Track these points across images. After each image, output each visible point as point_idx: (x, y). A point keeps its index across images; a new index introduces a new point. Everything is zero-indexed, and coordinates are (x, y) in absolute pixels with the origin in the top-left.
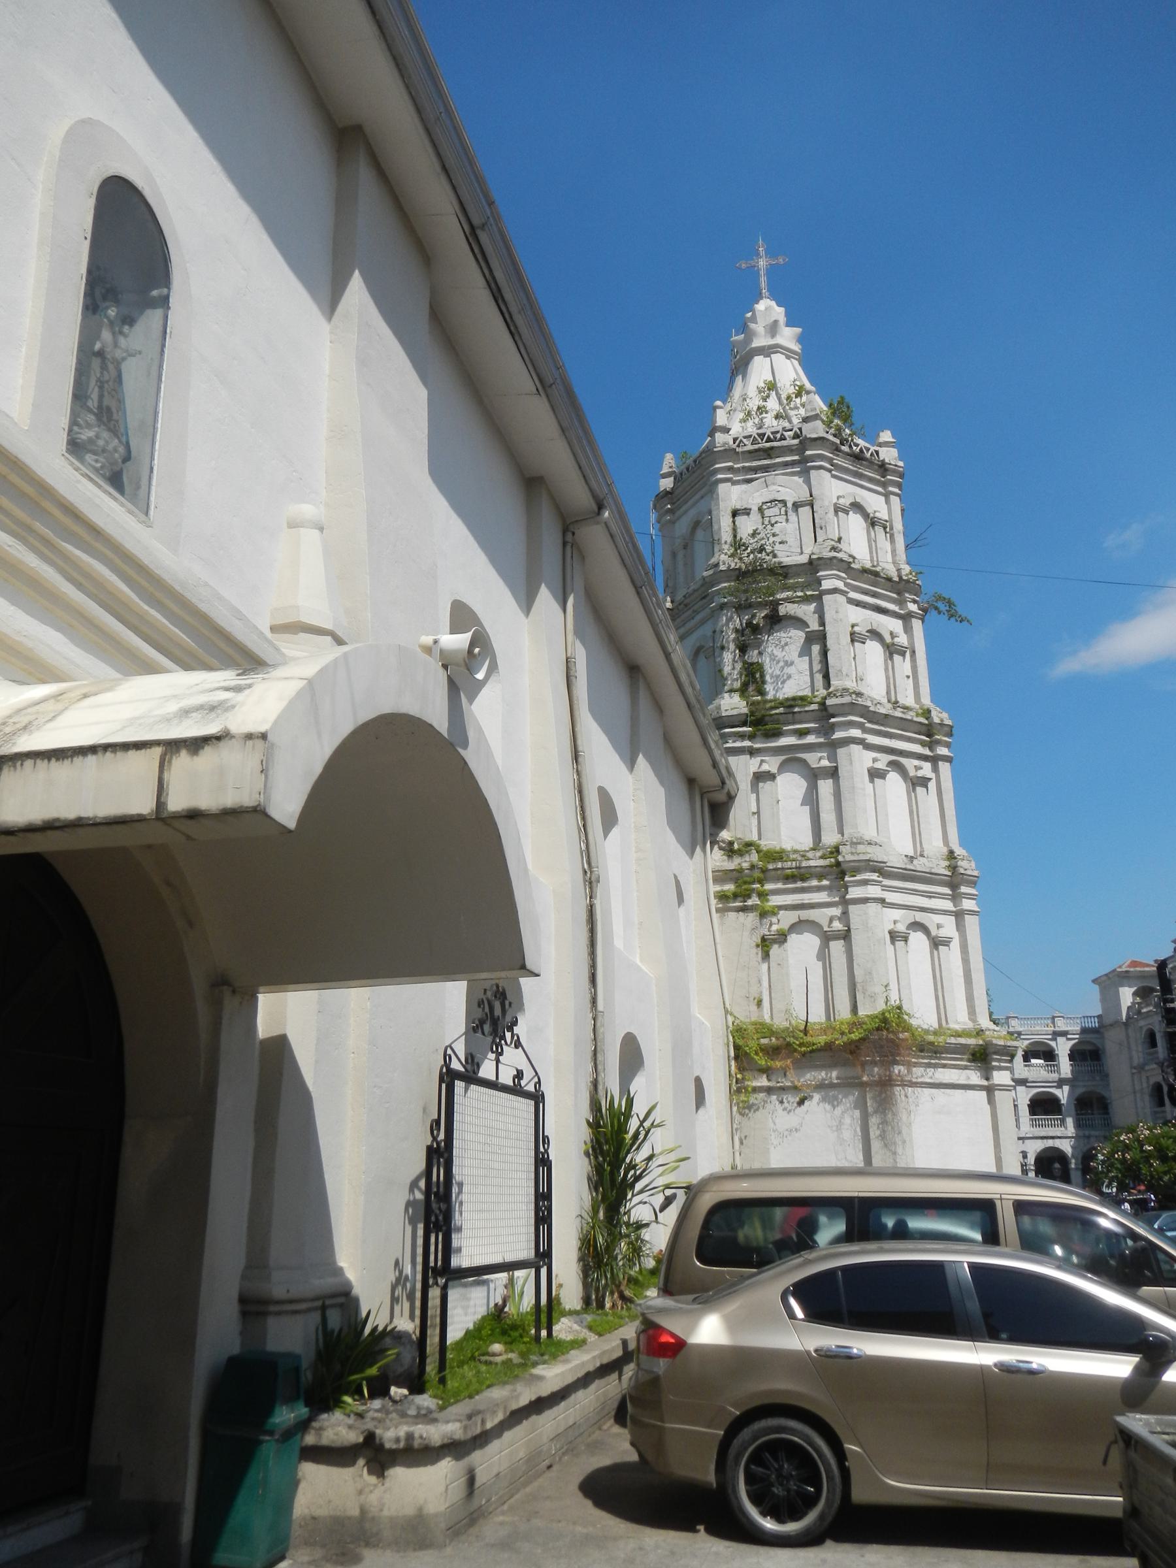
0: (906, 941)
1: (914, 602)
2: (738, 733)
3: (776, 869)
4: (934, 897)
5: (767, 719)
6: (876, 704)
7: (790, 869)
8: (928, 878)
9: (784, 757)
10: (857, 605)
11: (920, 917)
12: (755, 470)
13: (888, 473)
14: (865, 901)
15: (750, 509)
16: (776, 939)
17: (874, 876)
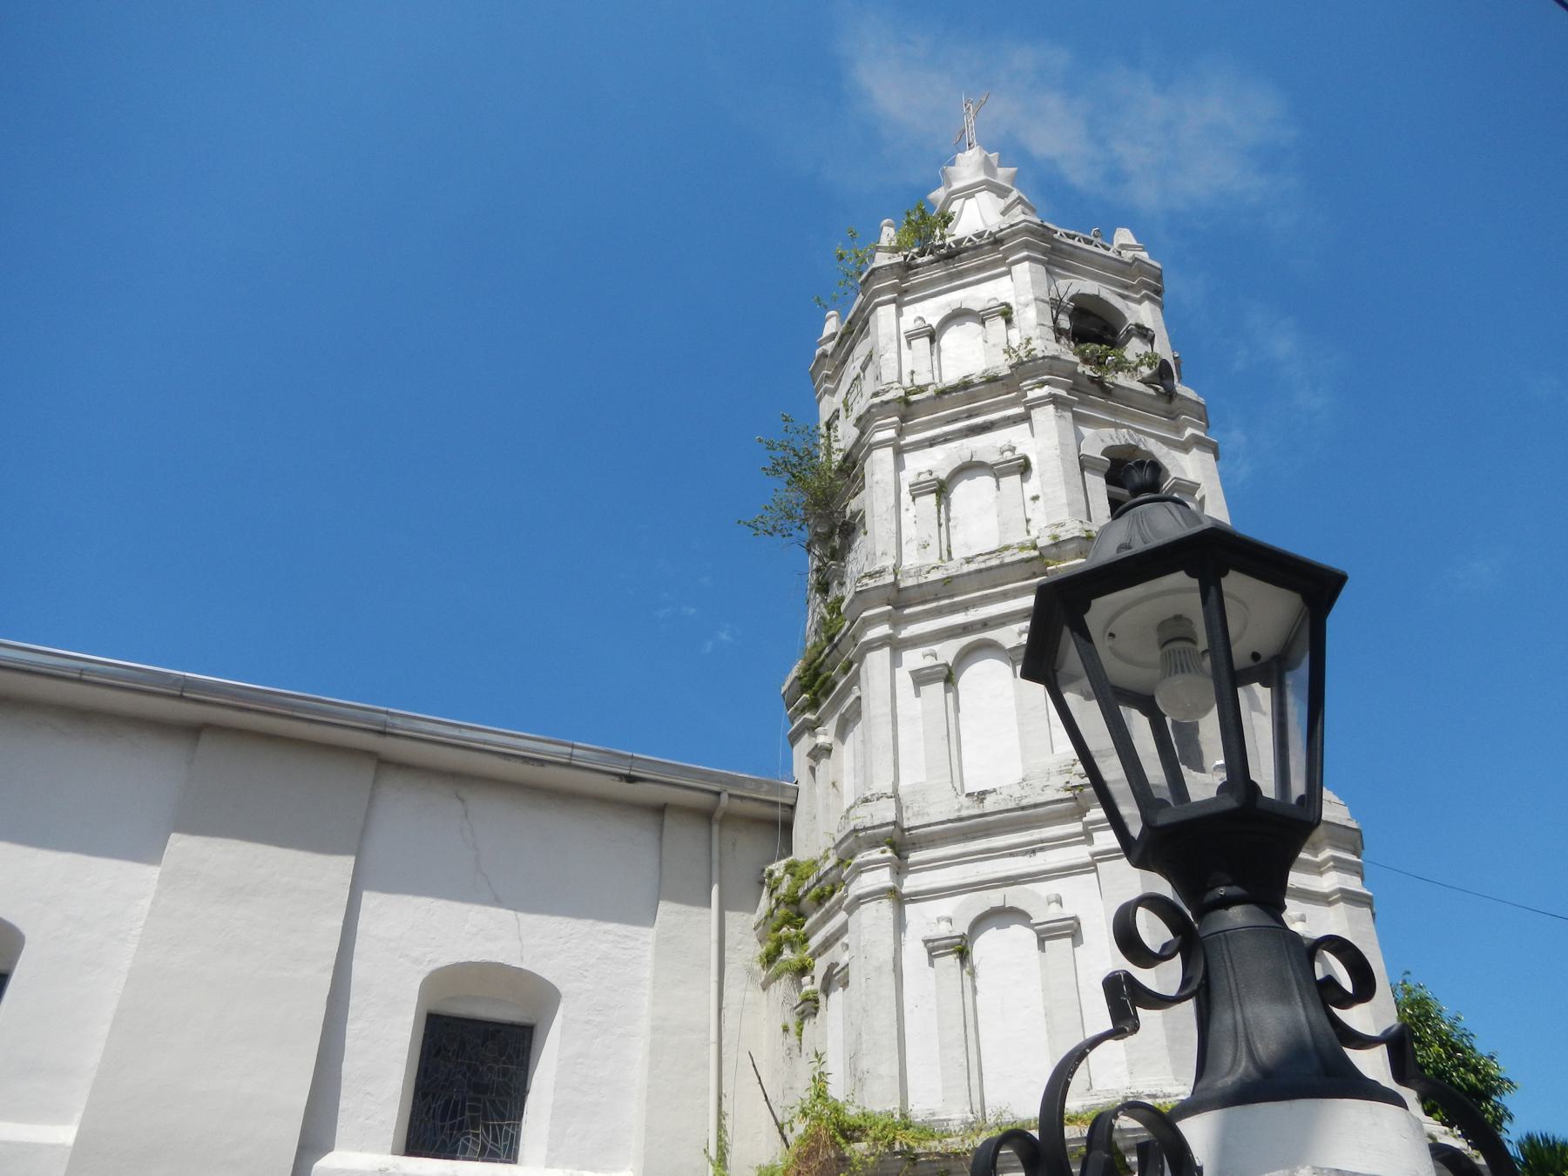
0: (963, 954)
1: (1043, 384)
2: (796, 709)
3: (806, 893)
4: (1042, 849)
5: (822, 670)
6: (928, 572)
7: (814, 885)
8: (1023, 817)
9: (837, 716)
10: (931, 446)
11: (995, 898)
12: (844, 362)
13: (1004, 242)
14: (859, 900)
15: (838, 411)
16: (803, 1012)
17: (875, 854)
